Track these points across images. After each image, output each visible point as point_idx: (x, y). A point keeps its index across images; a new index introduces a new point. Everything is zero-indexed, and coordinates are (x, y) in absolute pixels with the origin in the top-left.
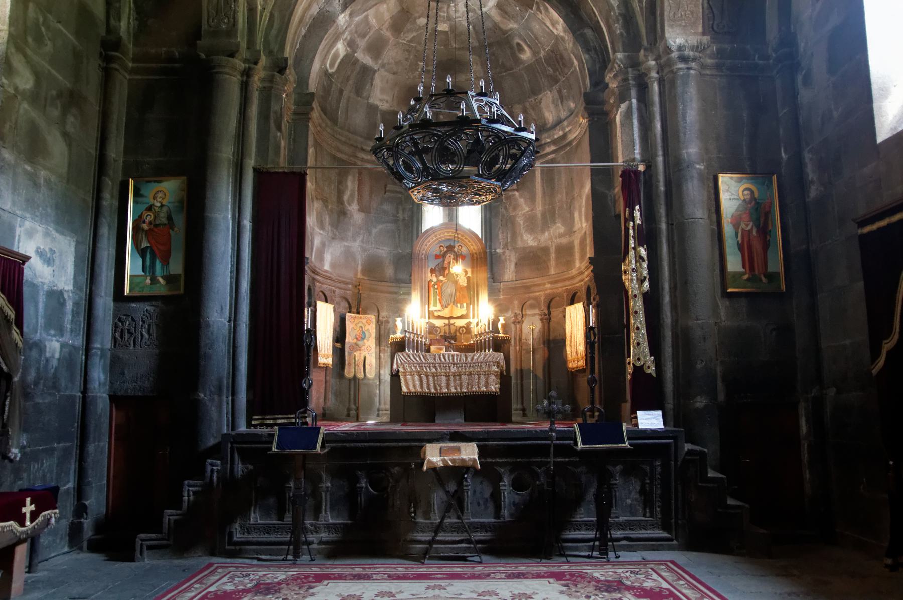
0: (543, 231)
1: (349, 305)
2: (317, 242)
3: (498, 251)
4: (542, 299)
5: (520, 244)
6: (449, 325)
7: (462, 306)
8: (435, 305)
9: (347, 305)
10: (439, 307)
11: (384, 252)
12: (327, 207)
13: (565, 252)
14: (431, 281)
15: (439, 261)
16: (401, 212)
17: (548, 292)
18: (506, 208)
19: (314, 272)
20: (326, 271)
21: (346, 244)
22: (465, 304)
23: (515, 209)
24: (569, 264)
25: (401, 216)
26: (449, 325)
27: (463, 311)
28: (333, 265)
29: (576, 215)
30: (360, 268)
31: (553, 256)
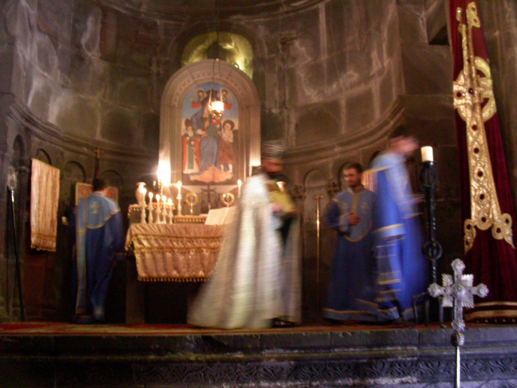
0: (330, 82)
1: (84, 172)
2: (37, 84)
3: (274, 111)
4: (331, 166)
5: (301, 101)
6: (209, 191)
7: (227, 169)
8: (191, 167)
9: (81, 173)
10: (196, 169)
11: (131, 111)
12: (56, 46)
13: (360, 104)
14: (186, 135)
15: (198, 109)
16: (154, 65)
17: (338, 157)
18: (283, 60)
19: (29, 120)
20: (51, 125)
21: (82, 96)
22: (231, 166)
23: (294, 59)
24: (366, 118)
25: (154, 69)
26: (209, 191)
27: (228, 175)
28: (60, 119)
29: (374, 54)
30: (98, 129)
31: (344, 110)
